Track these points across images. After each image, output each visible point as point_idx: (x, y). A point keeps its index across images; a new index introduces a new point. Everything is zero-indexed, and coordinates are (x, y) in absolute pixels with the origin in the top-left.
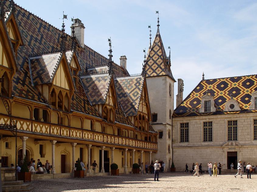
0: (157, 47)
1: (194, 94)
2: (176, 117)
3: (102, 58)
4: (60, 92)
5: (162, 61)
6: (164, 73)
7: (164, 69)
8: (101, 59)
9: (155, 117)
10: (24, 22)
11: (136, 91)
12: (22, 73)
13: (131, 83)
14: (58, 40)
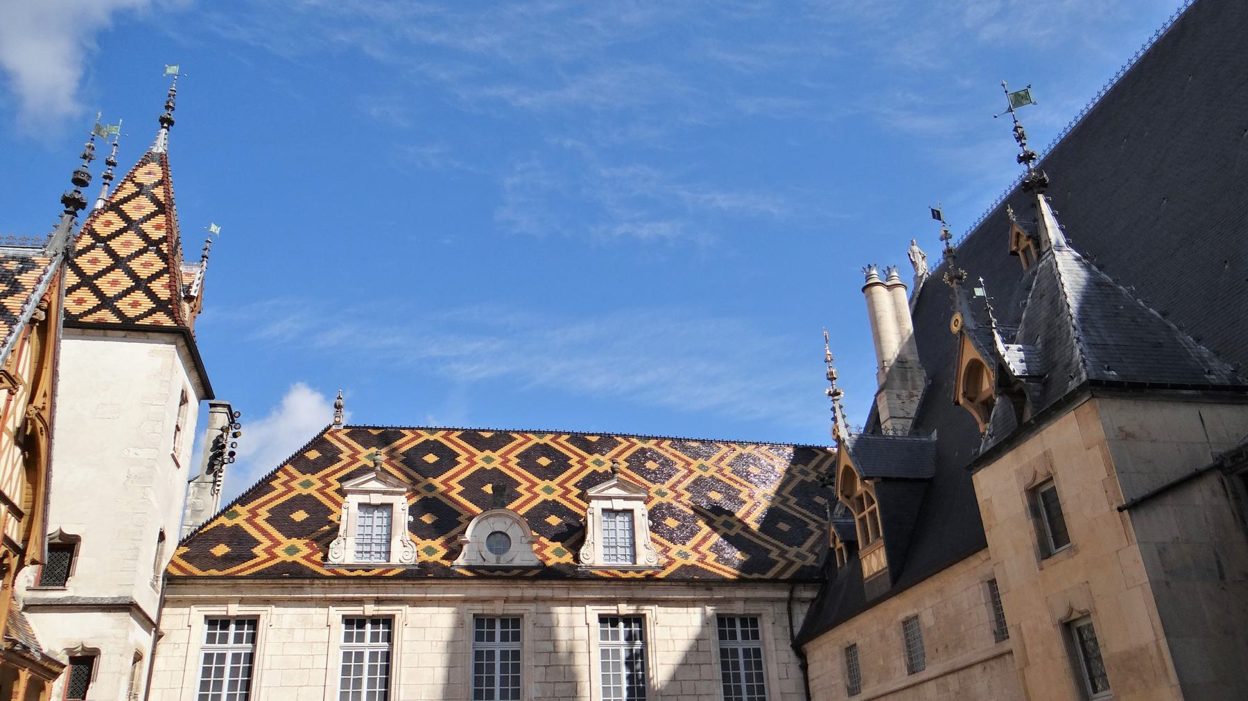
0: (143, 200)
1: (293, 478)
5: (159, 265)
6: (163, 319)
7: (170, 301)
9: (66, 547)
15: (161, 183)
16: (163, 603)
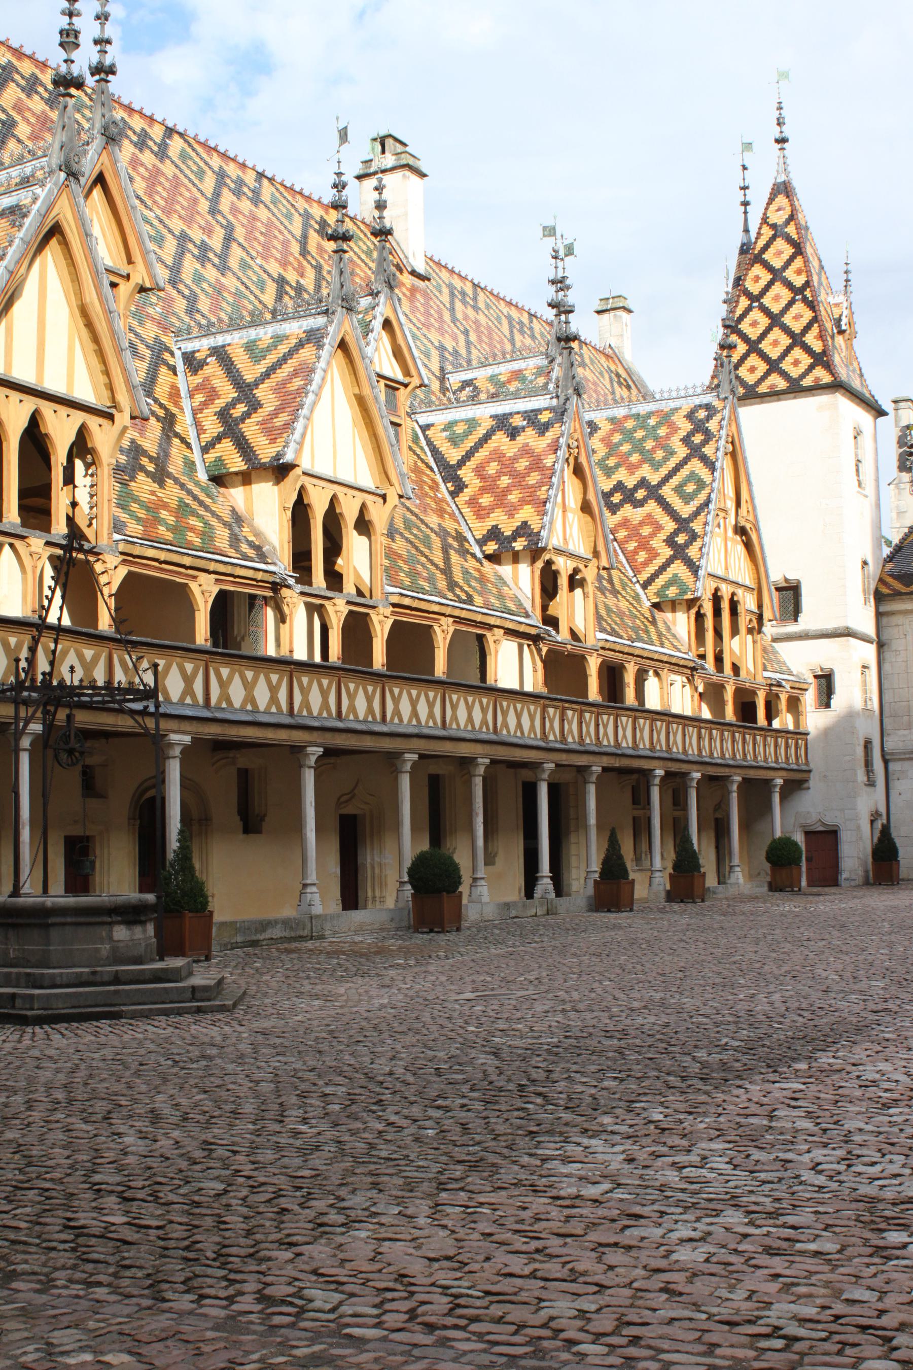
0: (780, 243)
2: (897, 595)
3: (514, 314)
4: (332, 500)
5: (808, 315)
7: (824, 352)
8: (509, 318)
9: (791, 594)
10: (146, 174)
11: (692, 473)
12: (153, 420)
13: (662, 432)
14: (304, 242)
15: (792, 218)
16: (879, 615)
